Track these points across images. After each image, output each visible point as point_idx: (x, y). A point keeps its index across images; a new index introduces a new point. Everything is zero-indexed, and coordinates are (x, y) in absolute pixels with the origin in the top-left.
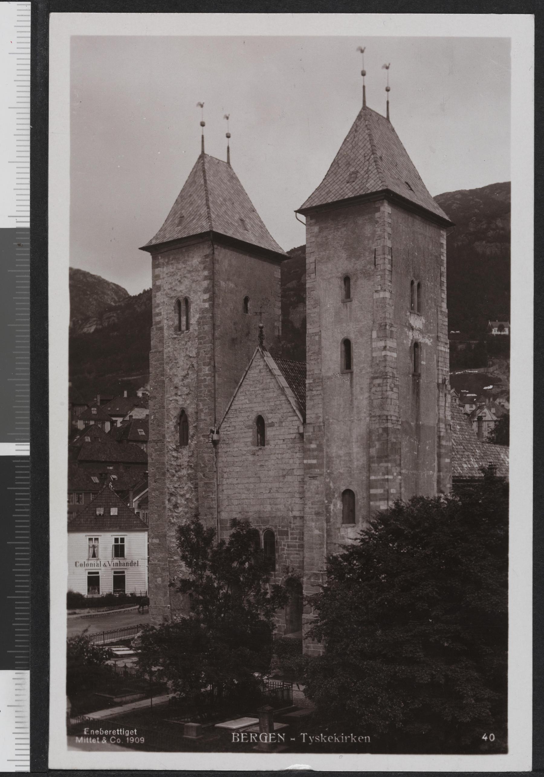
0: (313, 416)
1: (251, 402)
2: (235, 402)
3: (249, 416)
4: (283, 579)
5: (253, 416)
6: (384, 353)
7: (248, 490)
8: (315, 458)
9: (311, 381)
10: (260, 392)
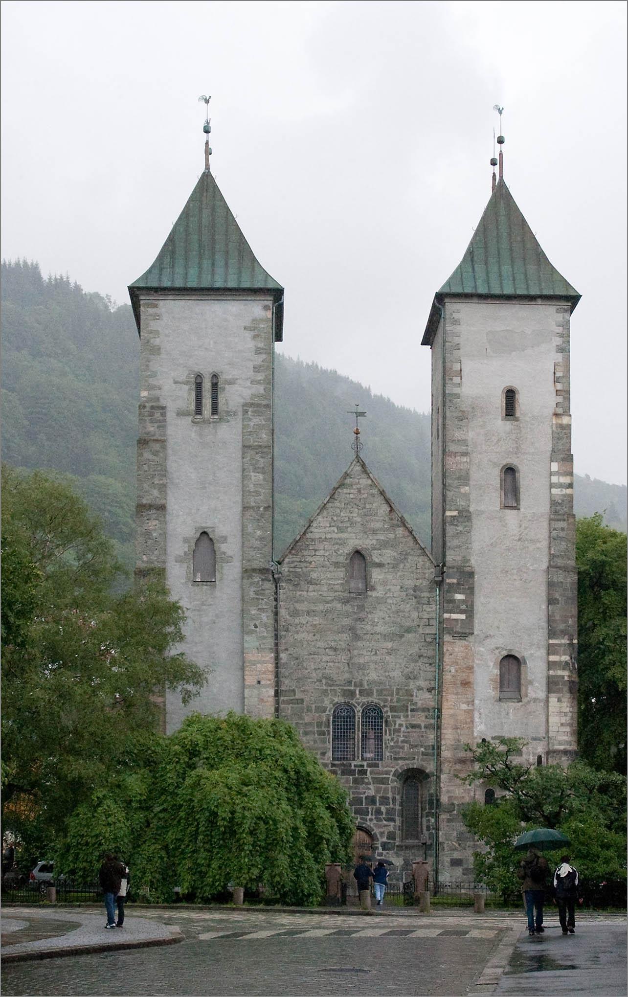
0: (459, 558)
1: (341, 530)
2: (312, 529)
3: (338, 550)
4: (397, 770)
5: (348, 549)
6: (569, 491)
7: (335, 650)
8: (461, 612)
9: (455, 513)
10: (359, 519)
